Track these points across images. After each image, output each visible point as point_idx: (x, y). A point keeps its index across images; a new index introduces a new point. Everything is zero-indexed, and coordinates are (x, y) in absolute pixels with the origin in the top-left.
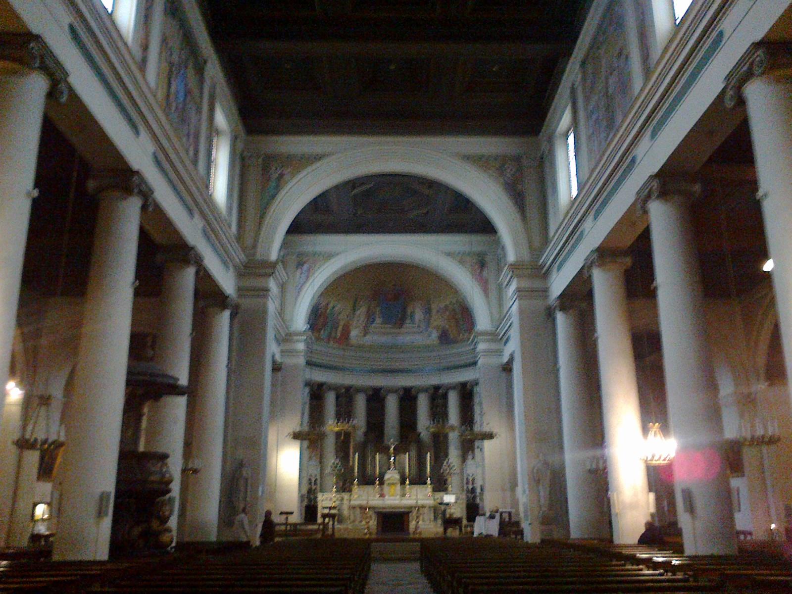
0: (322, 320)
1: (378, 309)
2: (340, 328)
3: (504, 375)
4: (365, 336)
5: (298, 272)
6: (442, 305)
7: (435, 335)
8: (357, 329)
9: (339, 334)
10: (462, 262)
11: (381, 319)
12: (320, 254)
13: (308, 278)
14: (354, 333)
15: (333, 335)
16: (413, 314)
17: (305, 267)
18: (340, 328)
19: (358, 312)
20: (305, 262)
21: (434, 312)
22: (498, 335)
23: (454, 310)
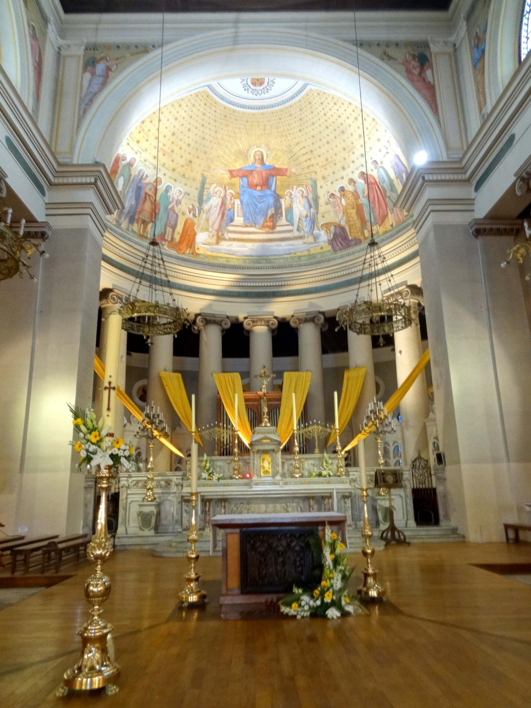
0: (148, 206)
1: (237, 202)
2: (179, 228)
3: (479, 242)
4: (217, 243)
5: (88, 76)
6: (335, 189)
7: (324, 237)
8: (206, 233)
9: (177, 237)
10: (387, 57)
11: (242, 219)
12: (128, 47)
13: (104, 84)
14: (201, 238)
15: (168, 237)
16: (290, 209)
17: (100, 67)
18: (179, 228)
19: (206, 207)
20: (98, 62)
21: (322, 202)
22: (463, 170)
23: (355, 195)
